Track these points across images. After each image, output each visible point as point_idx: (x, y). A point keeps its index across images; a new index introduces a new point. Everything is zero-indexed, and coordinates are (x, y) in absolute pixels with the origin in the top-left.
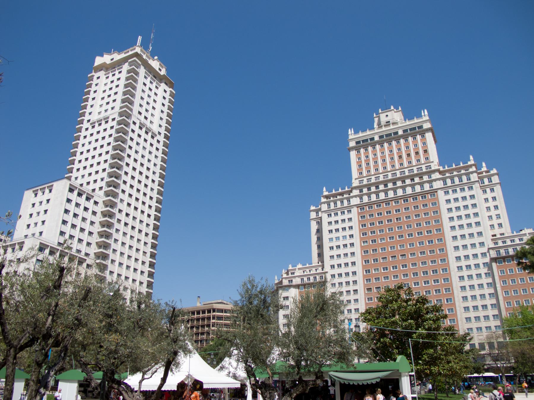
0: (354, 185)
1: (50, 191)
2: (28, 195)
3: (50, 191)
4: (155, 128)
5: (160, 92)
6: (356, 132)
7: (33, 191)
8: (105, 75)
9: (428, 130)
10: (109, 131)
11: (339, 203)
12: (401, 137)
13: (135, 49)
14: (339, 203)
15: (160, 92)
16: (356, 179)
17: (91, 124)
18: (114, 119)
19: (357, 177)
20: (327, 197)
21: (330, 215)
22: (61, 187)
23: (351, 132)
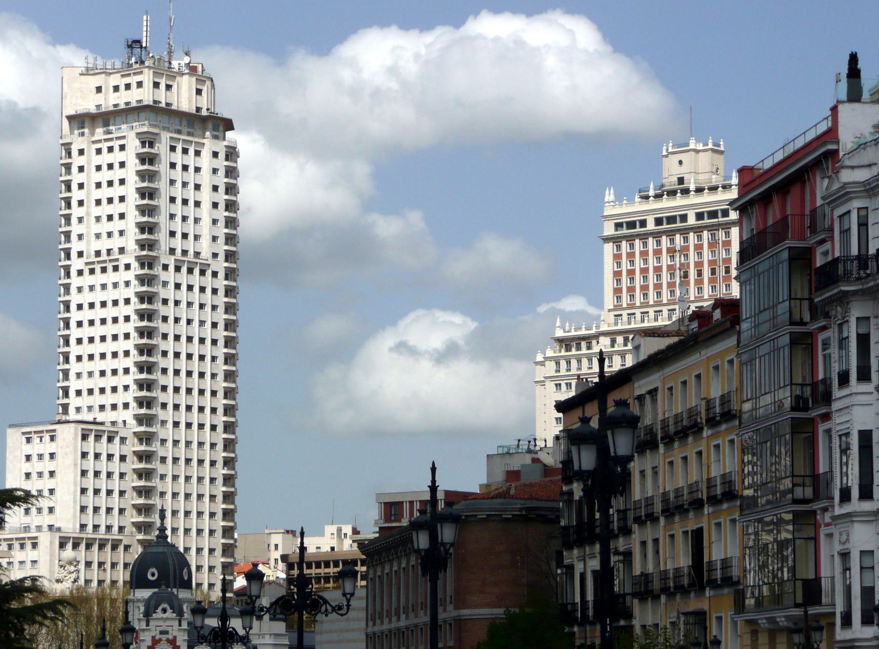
0: (604, 328)
1: (52, 438)
2: (14, 437)
3: (52, 438)
4: (205, 247)
5: (206, 161)
6: (619, 199)
7: (24, 433)
8: (94, 142)
9: (734, 223)
10: (125, 284)
11: (574, 363)
12: (693, 229)
13: (141, 73)
14: (574, 363)
15: (206, 161)
16: (610, 311)
17: (87, 264)
18: (128, 267)
19: (612, 307)
20: (560, 341)
21: (558, 386)
22: (68, 434)
23: (609, 196)
